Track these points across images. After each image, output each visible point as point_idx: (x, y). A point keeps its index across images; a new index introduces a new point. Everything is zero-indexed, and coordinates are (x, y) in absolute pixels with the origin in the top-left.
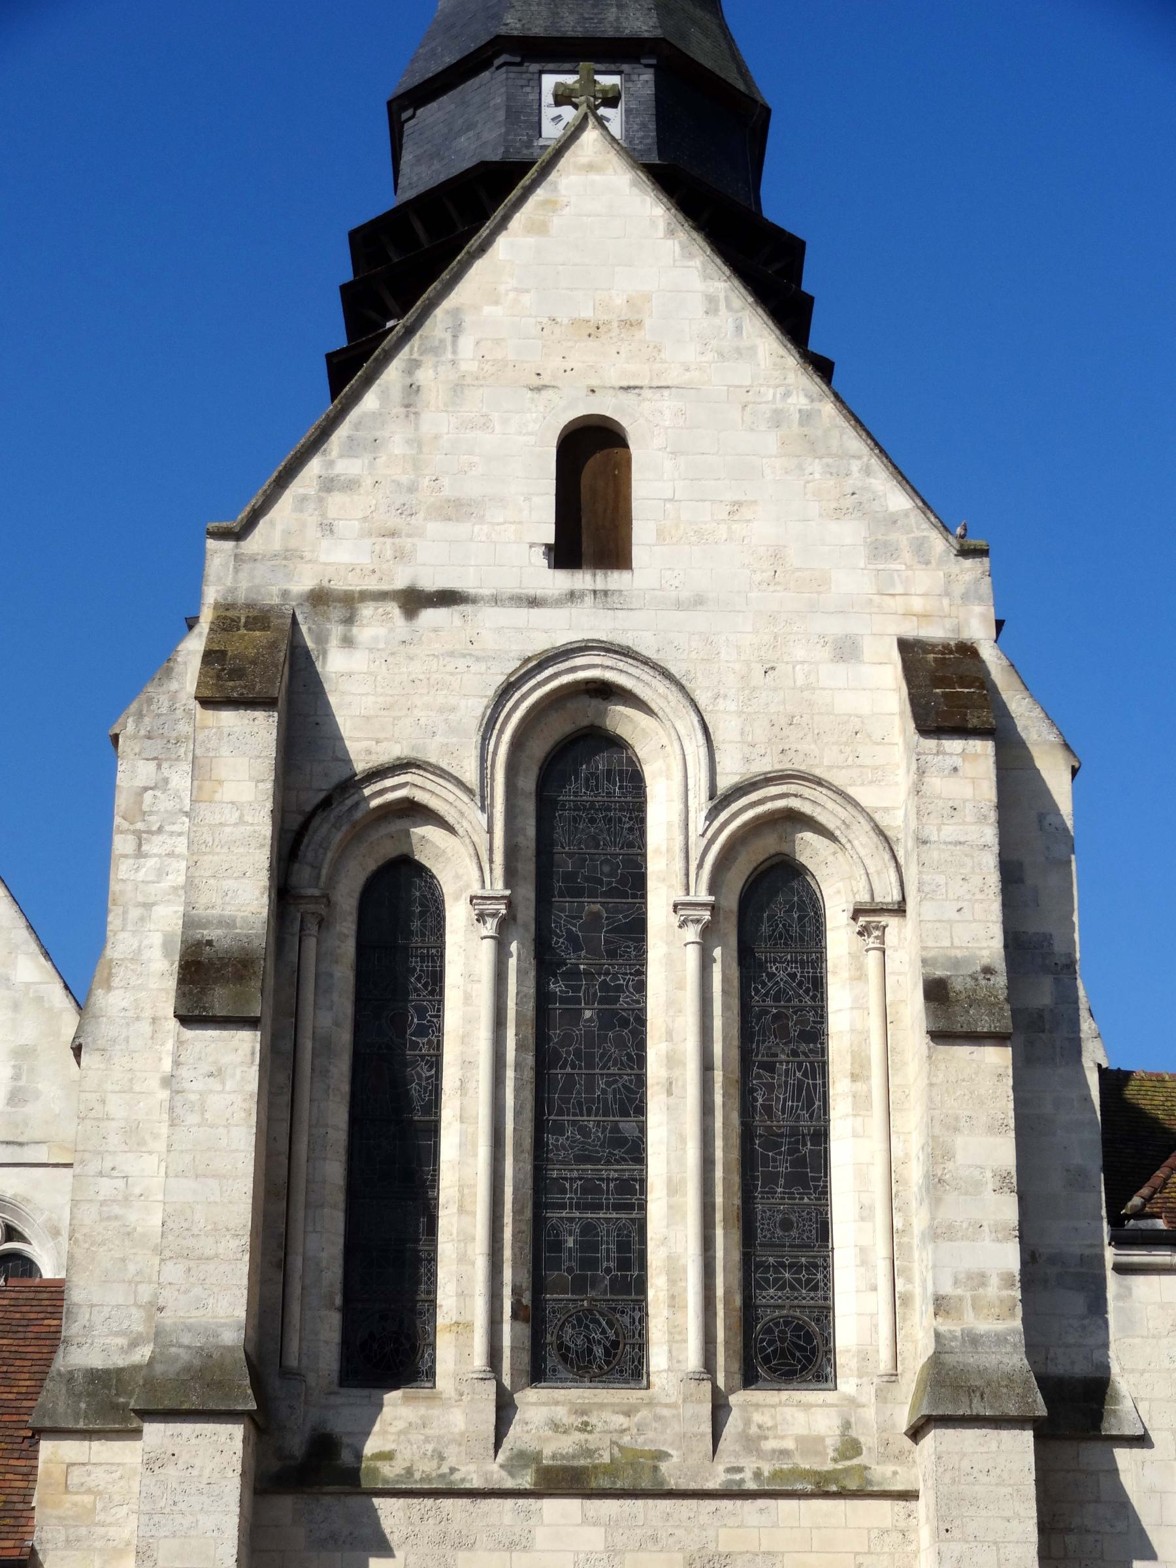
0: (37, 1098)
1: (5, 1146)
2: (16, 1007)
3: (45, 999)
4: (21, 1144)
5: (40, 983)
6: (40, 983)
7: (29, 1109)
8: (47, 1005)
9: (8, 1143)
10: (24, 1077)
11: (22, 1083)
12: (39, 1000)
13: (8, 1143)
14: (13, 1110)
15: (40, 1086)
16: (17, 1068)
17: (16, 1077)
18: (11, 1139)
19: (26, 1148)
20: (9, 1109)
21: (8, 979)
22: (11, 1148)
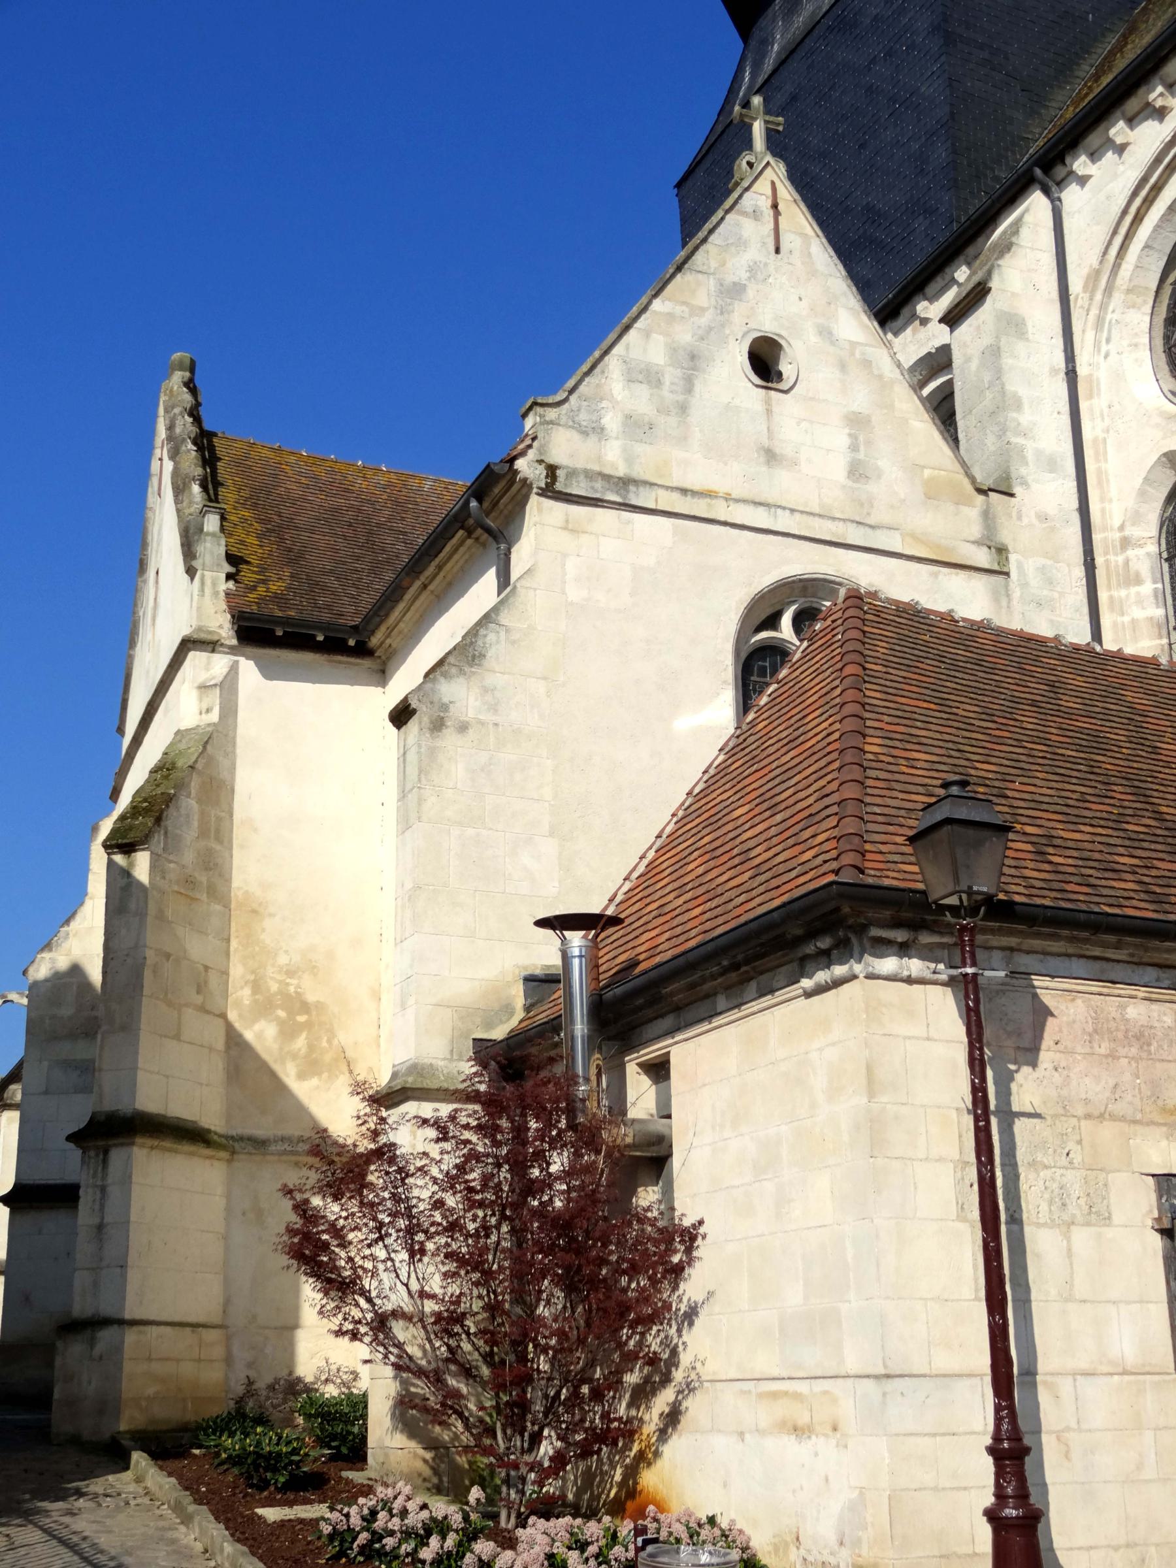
0: (879, 477)
1: (855, 525)
2: (843, 367)
3: (874, 364)
4: (872, 527)
5: (866, 345)
6: (866, 345)
7: (872, 488)
8: (876, 372)
9: (859, 523)
10: (862, 448)
11: (861, 456)
12: (867, 364)
13: (859, 523)
14: (855, 485)
15: (879, 463)
16: (853, 437)
17: (854, 448)
18: (858, 519)
19: (878, 532)
20: (850, 483)
21: (830, 333)
22: (862, 529)
